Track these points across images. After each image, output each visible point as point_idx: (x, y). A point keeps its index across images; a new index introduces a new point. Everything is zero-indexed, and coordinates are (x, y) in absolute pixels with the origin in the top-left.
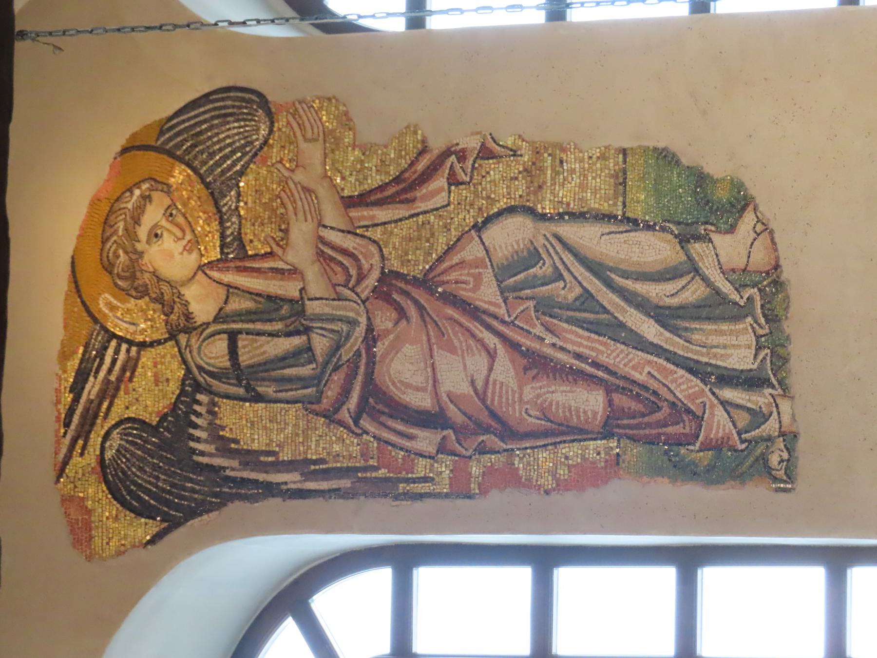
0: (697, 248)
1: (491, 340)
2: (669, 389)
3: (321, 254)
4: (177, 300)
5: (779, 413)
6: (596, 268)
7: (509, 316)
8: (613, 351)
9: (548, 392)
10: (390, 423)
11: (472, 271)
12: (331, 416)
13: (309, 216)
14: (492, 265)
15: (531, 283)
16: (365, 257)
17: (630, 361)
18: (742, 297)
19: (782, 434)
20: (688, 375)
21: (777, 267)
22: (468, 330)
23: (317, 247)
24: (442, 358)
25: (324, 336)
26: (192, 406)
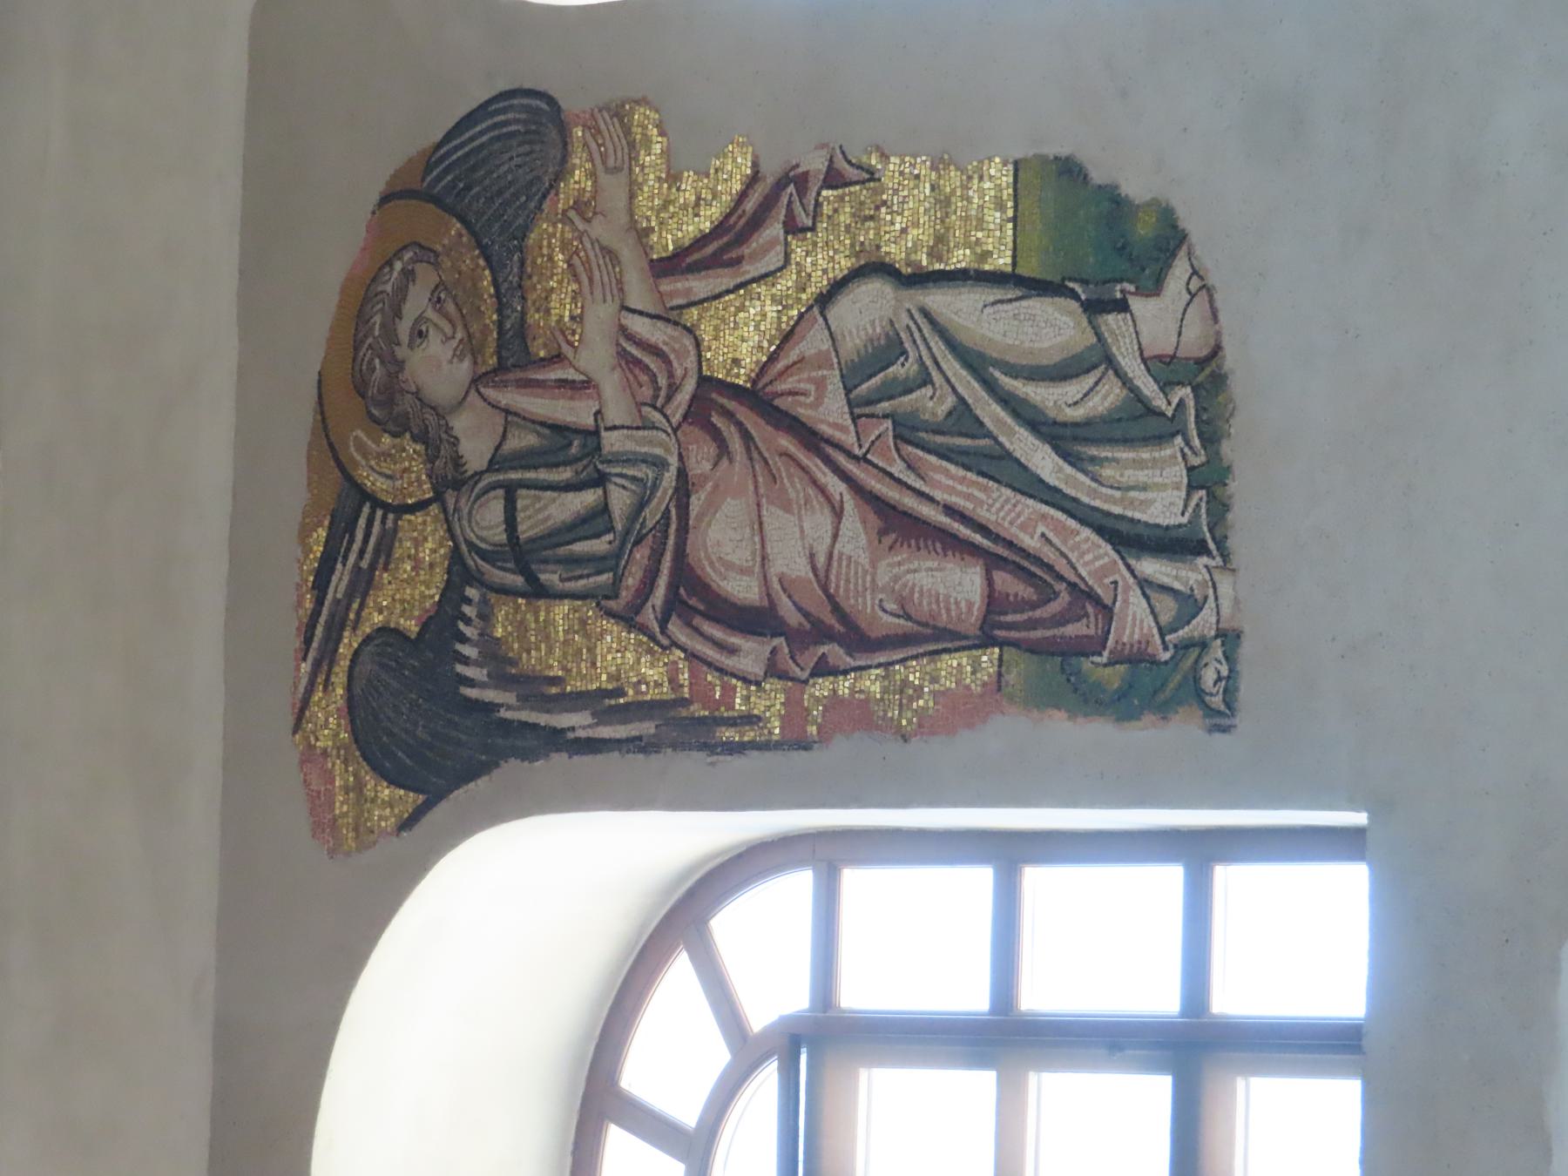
0: (1112, 320)
1: (836, 486)
2: (1069, 562)
3: (623, 354)
4: (444, 436)
5: (1216, 599)
6: (975, 362)
7: (860, 446)
8: (995, 500)
9: (908, 571)
10: (709, 628)
11: (814, 374)
12: (628, 619)
13: (609, 297)
14: (839, 363)
15: (887, 393)
16: (678, 358)
17: (1019, 516)
18: (1169, 403)
19: (1221, 634)
20: (1094, 537)
21: (1217, 350)
22: (803, 469)
23: (618, 344)
24: (774, 518)
25: (624, 487)
26: (460, 607)
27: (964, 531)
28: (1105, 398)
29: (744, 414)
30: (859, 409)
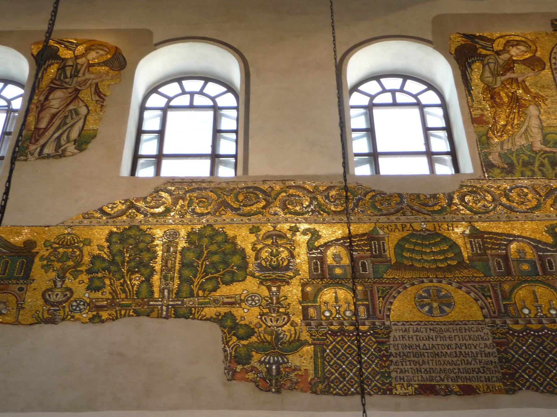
0: (73, 143)
1: (61, 108)
19: (27, 159)
24: (59, 100)
27: (50, 125)
28: (63, 142)
29: (74, 96)
30: (71, 111)
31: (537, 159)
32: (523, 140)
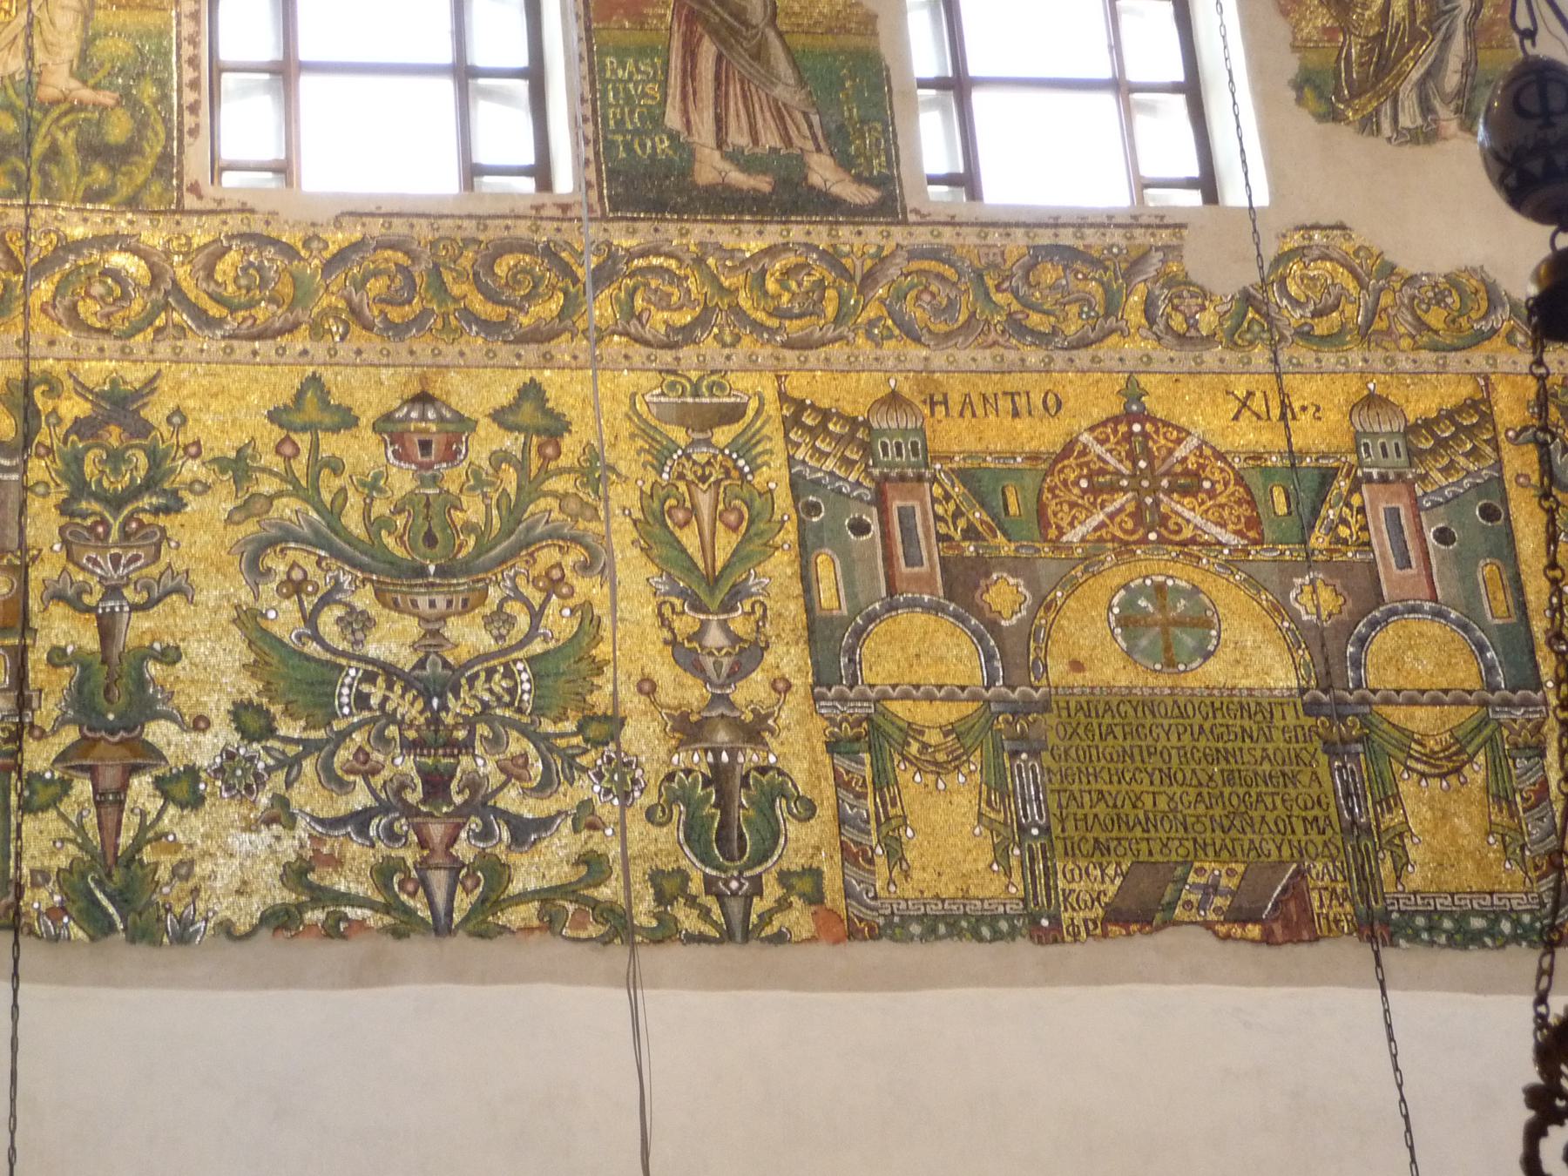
31: (43, 130)
32: (15, 56)
